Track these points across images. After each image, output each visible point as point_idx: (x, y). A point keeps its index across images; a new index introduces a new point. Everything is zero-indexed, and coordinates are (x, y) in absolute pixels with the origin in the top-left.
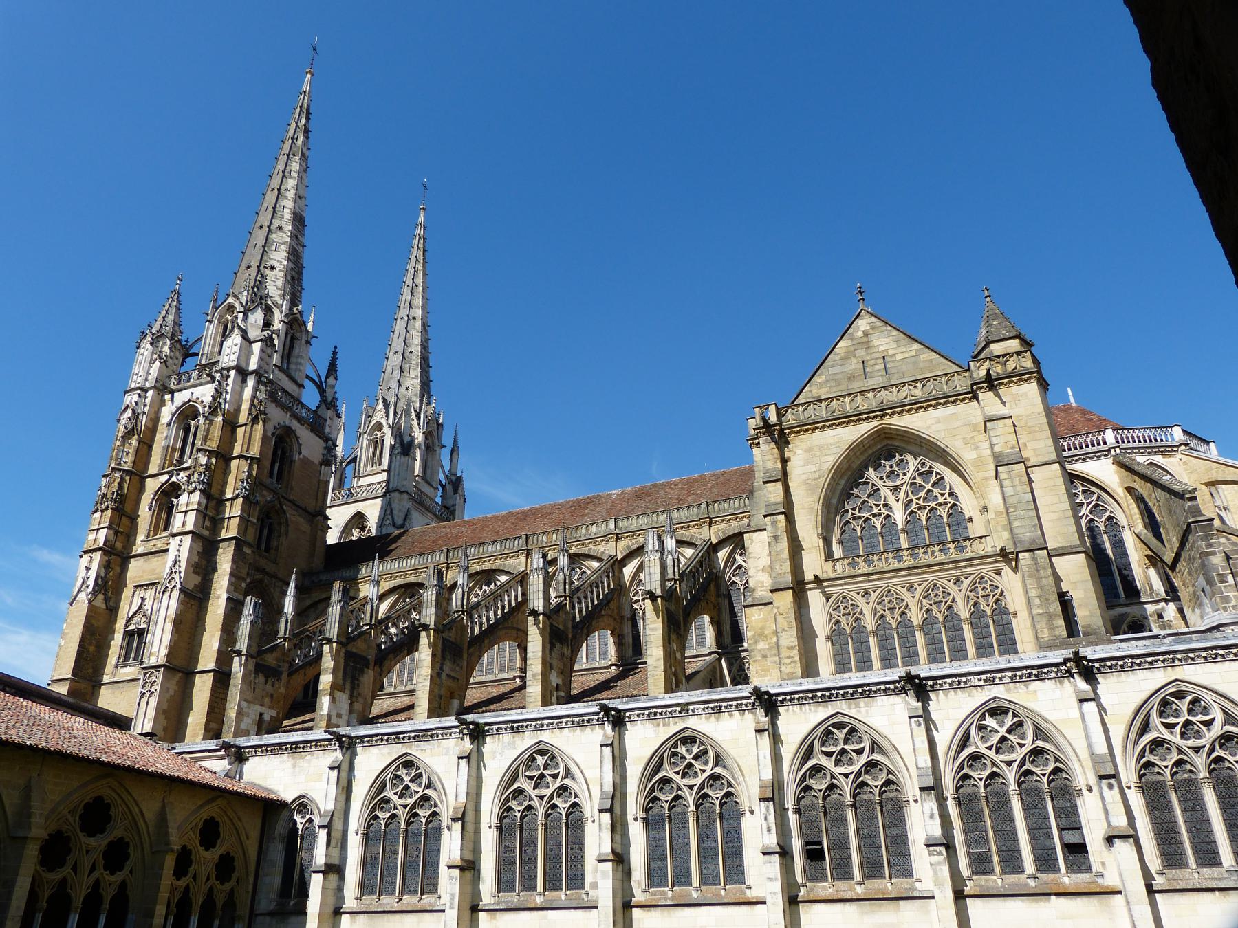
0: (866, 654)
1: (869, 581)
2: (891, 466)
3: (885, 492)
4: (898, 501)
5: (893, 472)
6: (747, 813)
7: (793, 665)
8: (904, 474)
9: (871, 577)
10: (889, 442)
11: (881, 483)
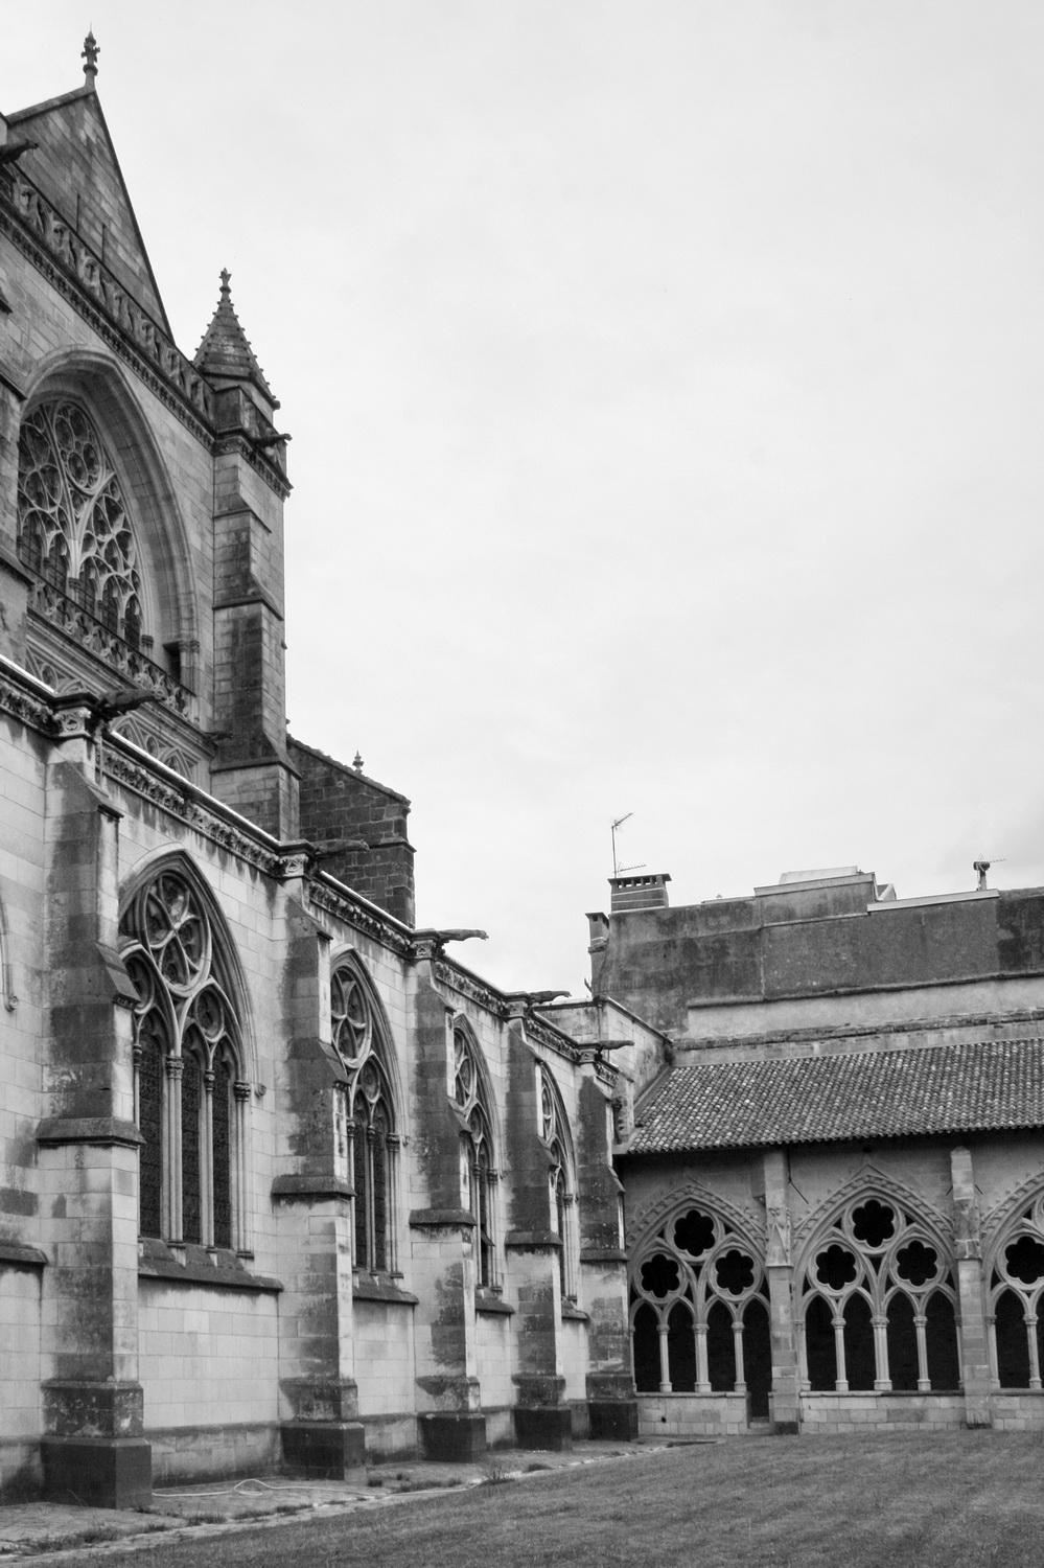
3: (62, 485)
10: (85, 399)
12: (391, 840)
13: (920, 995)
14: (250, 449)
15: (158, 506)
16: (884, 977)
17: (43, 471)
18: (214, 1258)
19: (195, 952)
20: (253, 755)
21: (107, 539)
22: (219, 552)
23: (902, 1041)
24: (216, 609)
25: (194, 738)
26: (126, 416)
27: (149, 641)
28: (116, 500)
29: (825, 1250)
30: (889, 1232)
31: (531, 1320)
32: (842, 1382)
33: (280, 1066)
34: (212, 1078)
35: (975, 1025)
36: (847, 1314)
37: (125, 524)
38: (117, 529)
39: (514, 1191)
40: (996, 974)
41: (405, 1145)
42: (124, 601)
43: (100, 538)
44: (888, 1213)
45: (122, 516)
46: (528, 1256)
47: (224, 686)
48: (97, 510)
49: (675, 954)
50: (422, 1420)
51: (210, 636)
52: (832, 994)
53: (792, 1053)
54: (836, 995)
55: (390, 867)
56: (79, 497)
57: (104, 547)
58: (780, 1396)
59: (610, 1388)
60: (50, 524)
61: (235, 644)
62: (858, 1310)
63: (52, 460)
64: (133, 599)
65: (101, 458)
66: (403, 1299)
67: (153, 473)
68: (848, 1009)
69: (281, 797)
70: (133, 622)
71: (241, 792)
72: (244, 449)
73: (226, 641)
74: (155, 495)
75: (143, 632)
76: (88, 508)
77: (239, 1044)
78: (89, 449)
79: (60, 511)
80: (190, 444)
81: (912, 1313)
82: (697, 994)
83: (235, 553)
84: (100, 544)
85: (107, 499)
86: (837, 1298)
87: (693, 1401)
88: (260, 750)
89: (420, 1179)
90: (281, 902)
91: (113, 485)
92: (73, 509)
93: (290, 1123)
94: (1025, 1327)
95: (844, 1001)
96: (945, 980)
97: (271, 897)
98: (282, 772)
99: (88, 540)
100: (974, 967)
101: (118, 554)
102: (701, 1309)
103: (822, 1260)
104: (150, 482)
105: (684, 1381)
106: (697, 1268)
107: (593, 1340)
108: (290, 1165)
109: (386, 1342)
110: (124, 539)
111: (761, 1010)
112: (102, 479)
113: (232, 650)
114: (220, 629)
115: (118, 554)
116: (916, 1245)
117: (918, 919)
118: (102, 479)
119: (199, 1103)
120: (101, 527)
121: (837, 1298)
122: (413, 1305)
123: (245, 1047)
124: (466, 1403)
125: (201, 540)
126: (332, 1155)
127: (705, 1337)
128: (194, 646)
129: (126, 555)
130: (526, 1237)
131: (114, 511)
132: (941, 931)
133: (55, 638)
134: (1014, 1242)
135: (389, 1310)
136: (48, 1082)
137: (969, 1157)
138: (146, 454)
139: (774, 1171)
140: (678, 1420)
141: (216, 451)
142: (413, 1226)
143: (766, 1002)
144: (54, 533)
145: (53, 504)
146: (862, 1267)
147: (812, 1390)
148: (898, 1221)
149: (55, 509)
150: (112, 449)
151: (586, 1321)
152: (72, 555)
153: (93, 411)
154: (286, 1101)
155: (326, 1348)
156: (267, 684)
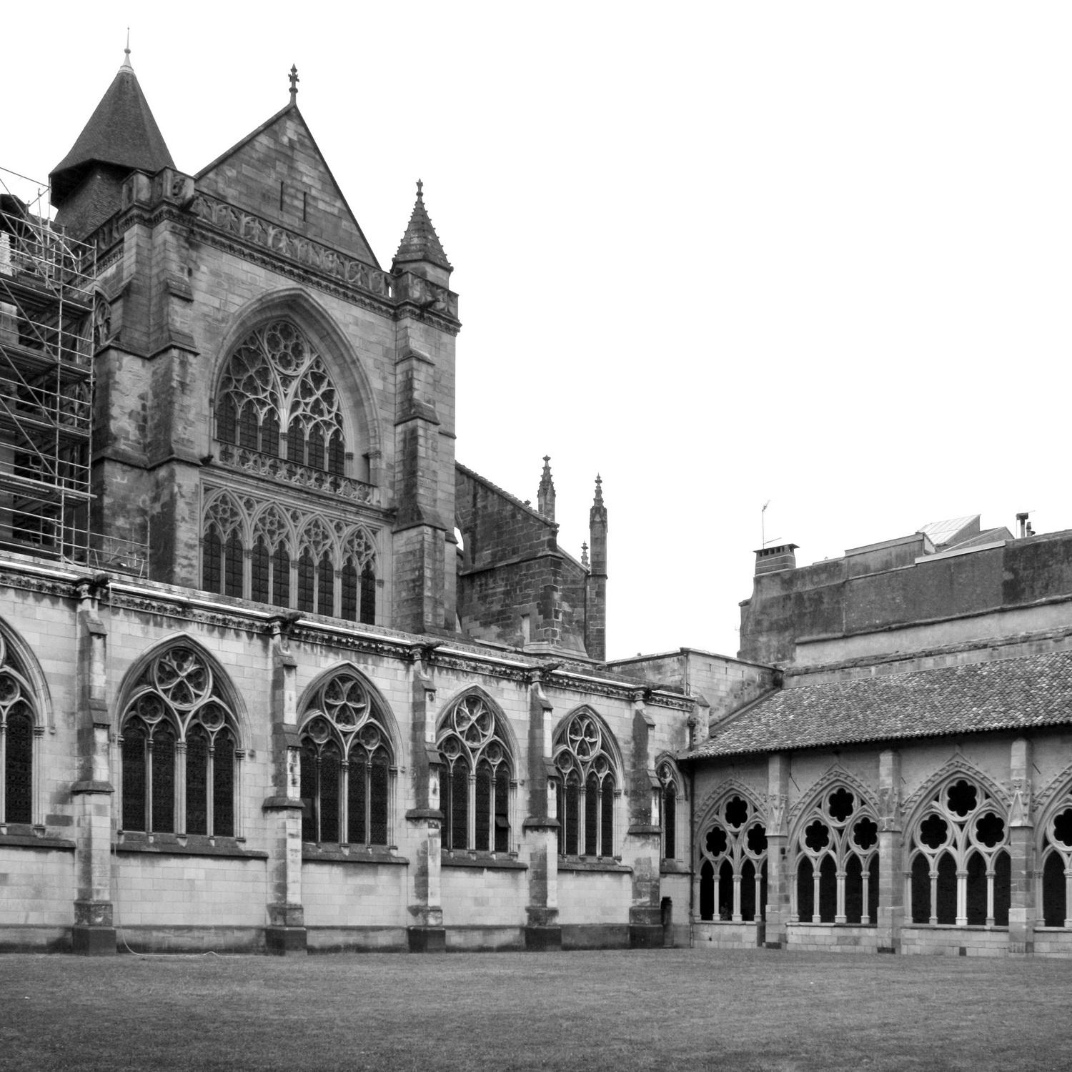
0: (237, 577)
1: (257, 488)
2: (286, 347)
3: (274, 377)
4: (286, 395)
5: (285, 355)
6: (247, 758)
7: (190, 569)
8: (297, 365)
9: (261, 484)
10: (291, 315)
11: (272, 362)
12: (544, 553)
13: (947, 626)
14: (418, 311)
15: (350, 369)
16: (924, 613)
17: (258, 372)
18: (213, 842)
19: (199, 686)
20: (412, 519)
21: (311, 400)
22: (398, 386)
23: (929, 663)
24: (396, 425)
25: (376, 515)
26: (317, 319)
27: (350, 456)
28: (321, 371)
29: (811, 824)
30: (972, 805)
31: (536, 872)
32: (816, 916)
33: (269, 739)
34: (212, 750)
35: (979, 648)
36: (822, 869)
37: (329, 384)
38: (324, 388)
39: (531, 792)
40: (998, 608)
41: (403, 772)
42: (328, 435)
43: (307, 401)
44: (973, 791)
45: (326, 380)
46: (536, 833)
47: (399, 476)
48: (304, 383)
49: (790, 604)
50: (408, 930)
51: (390, 446)
52: (888, 629)
53: (857, 675)
54: (890, 630)
55: (542, 572)
56: (286, 380)
57: (310, 406)
58: (770, 925)
59: (642, 917)
60: (262, 403)
61: (405, 447)
62: (828, 864)
63: (264, 361)
64: (337, 433)
65: (306, 348)
66: (394, 861)
67: (343, 349)
68: (898, 640)
69: (426, 545)
70: (337, 444)
71: (406, 544)
72: (413, 313)
73: (400, 446)
74: (345, 361)
75: (347, 450)
76: (295, 384)
77: (237, 730)
78: (297, 345)
79: (272, 394)
80: (372, 320)
81: (811, 870)
82: (802, 635)
83: (405, 387)
84: (306, 404)
85: (312, 373)
86: (933, 855)
87: (727, 927)
88: (415, 518)
89: (412, 791)
90: (271, 648)
91: (318, 363)
92: (282, 389)
93: (271, 769)
94: (929, 880)
95: (896, 634)
96: (963, 614)
97: (266, 646)
98: (428, 530)
99: (295, 406)
100: (985, 603)
101: (324, 406)
102: (737, 865)
103: (810, 831)
104: (342, 355)
105: (727, 914)
106: (736, 835)
107: (635, 884)
108: (271, 792)
109: (377, 886)
110: (328, 396)
111: (842, 644)
112: (308, 361)
113: (403, 451)
114: (399, 438)
115: (324, 406)
116: (990, 816)
117: (949, 566)
118: (308, 361)
119: (206, 763)
120: (306, 391)
121: (933, 855)
122: (406, 864)
123: (241, 731)
124: (427, 921)
125: (381, 382)
126: (285, 785)
127: (739, 883)
128: (378, 454)
129: (331, 405)
130: (534, 821)
131: (318, 379)
132: (964, 576)
133: (250, 481)
134: (927, 818)
135: (380, 868)
136: (77, 764)
137: (891, 757)
138: (335, 338)
139: (775, 768)
140: (718, 940)
141: (396, 318)
142: (408, 818)
143: (845, 637)
144: (266, 409)
145: (264, 390)
146: (833, 836)
147: (801, 921)
148: (979, 799)
149: (268, 393)
150: (315, 340)
151: (630, 873)
152: (282, 419)
153: (298, 320)
154: (271, 758)
155: (282, 888)
156: (423, 472)
